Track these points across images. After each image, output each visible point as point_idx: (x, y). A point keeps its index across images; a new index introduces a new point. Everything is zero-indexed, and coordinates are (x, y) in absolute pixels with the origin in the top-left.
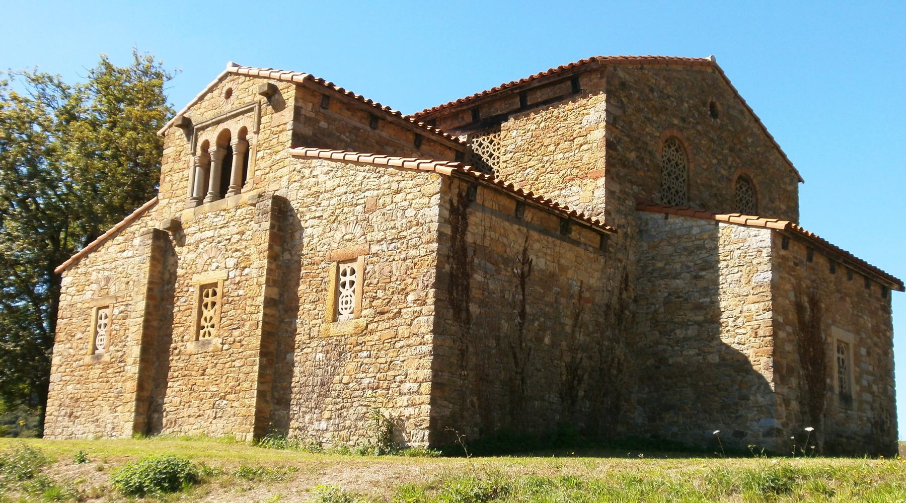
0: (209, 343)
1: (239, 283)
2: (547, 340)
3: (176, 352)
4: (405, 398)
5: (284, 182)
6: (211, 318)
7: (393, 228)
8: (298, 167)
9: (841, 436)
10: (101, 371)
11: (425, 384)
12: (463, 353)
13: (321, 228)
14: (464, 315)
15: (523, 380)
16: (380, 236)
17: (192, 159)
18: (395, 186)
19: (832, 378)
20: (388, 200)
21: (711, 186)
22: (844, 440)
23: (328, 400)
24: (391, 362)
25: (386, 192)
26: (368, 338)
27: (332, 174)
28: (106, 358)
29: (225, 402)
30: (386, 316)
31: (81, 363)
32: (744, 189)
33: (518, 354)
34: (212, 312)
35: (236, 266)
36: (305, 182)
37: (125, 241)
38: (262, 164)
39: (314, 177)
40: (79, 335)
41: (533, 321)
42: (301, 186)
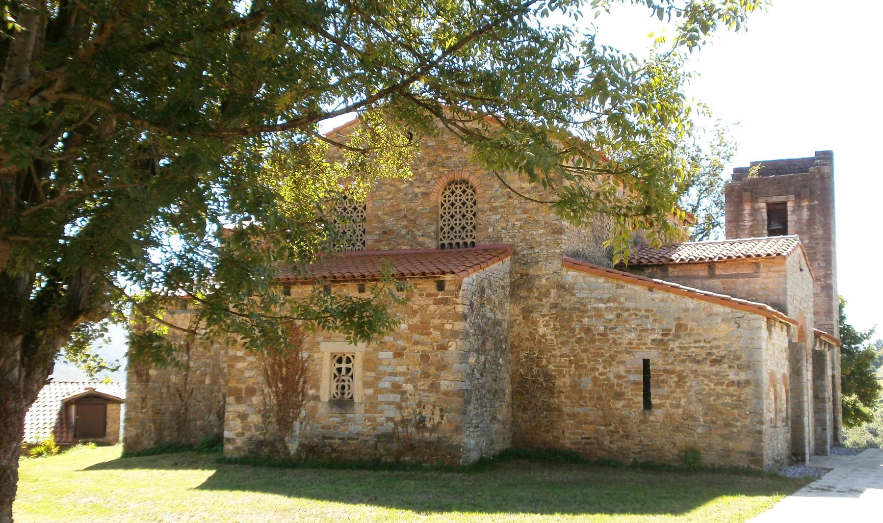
2: (207, 381)
9: (330, 438)
12: (144, 400)
14: (144, 377)
15: (186, 409)
19: (317, 387)
21: (399, 211)
22: (337, 441)
32: (458, 192)
33: (183, 394)
41: (196, 371)
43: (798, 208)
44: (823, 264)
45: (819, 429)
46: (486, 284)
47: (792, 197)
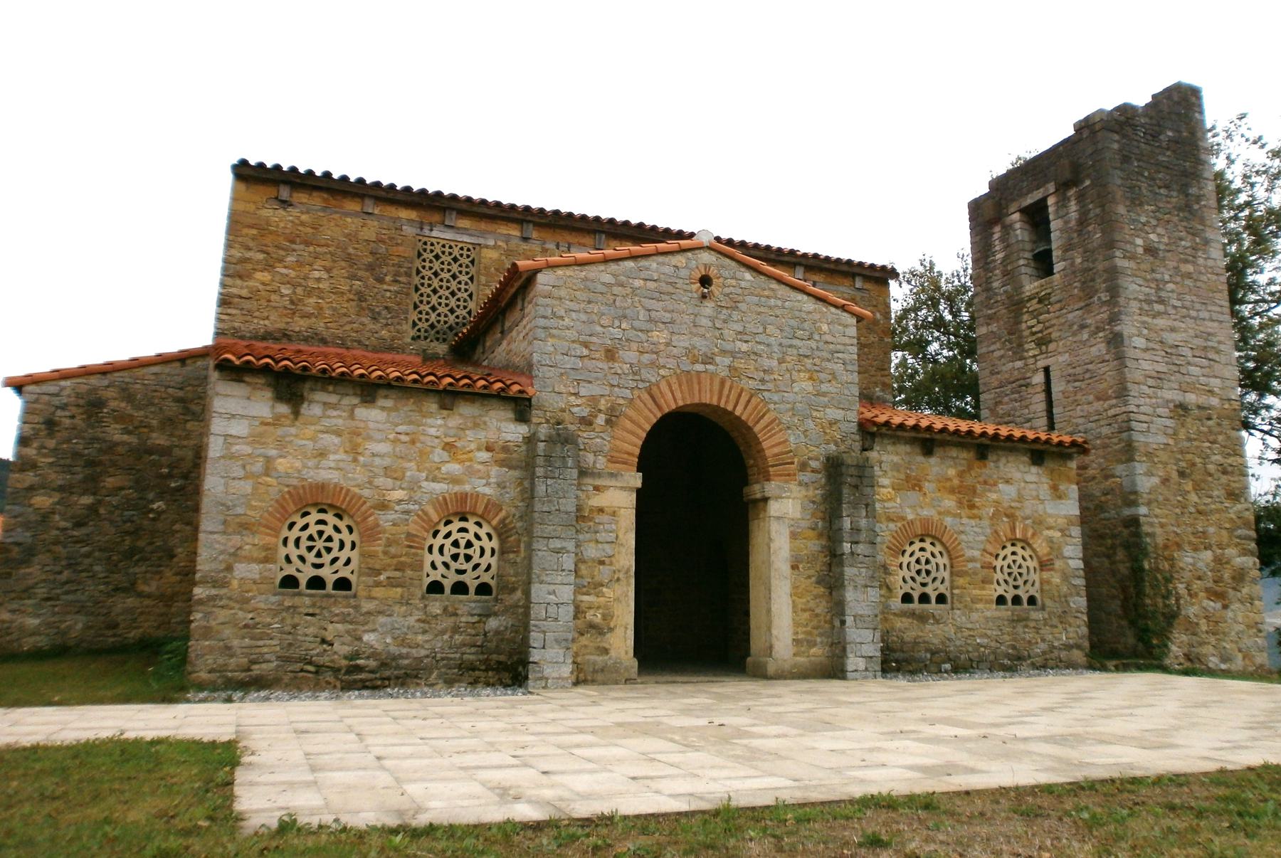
43: (1063, 203)
44: (1105, 297)
45: (837, 623)
46: (110, 393)
47: (1051, 187)
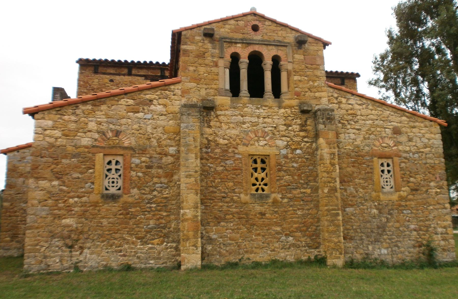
0: (267, 196)
1: (291, 158)
3: (228, 199)
4: (439, 236)
5: (324, 101)
6: (263, 179)
7: (414, 146)
8: (336, 95)
10: (121, 209)
11: (449, 229)
13: (362, 136)
16: (408, 149)
17: (221, 63)
18: (412, 124)
20: (409, 130)
23: (385, 237)
24: (427, 217)
25: (406, 125)
26: (408, 203)
27: (364, 106)
28: (125, 198)
29: (291, 238)
30: (419, 192)
31: (84, 199)
34: (263, 175)
35: (287, 147)
36: (342, 106)
37: (137, 104)
38: (301, 85)
39: (349, 104)
40: (76, 175)
42: (339, 107)
